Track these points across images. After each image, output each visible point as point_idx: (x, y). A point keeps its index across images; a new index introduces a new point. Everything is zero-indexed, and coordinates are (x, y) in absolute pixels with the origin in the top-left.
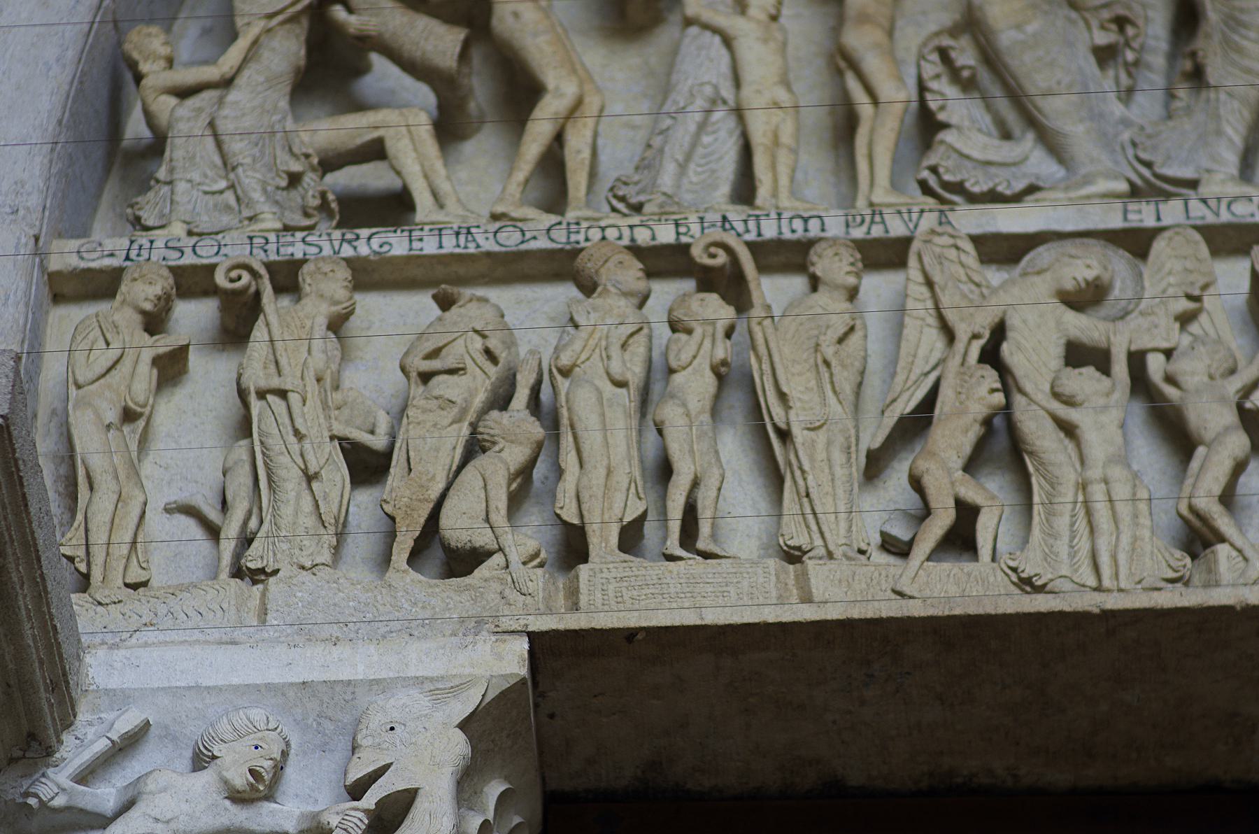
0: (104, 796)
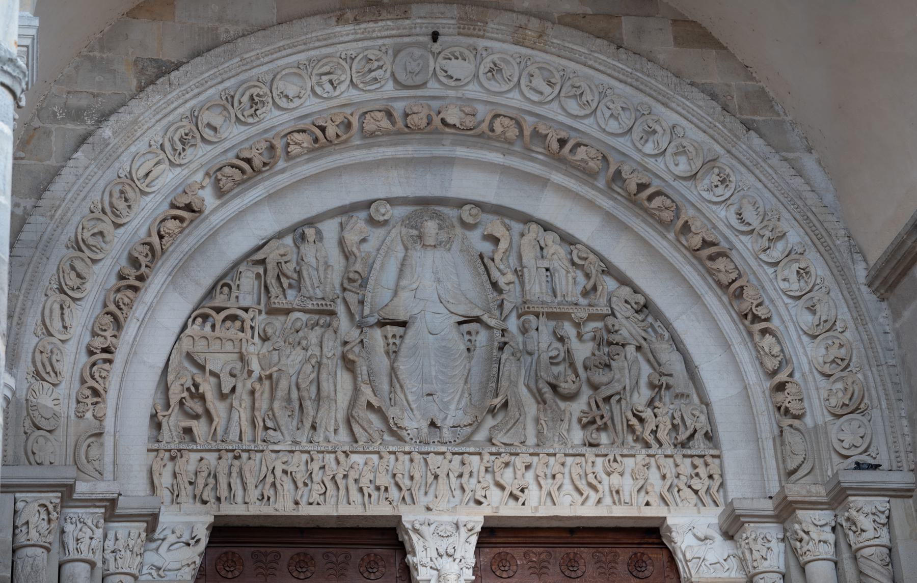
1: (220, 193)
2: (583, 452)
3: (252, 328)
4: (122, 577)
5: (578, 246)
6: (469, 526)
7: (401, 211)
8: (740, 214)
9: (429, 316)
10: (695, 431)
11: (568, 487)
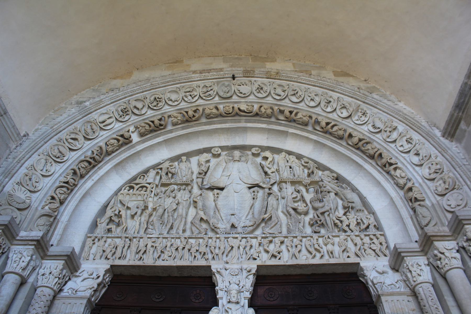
0: (81, 275)
1: (142, 135)
2: (312, 235)
3: (152, 191)
5: (304, 159)
6: (248, 269)
11: (304, 251)
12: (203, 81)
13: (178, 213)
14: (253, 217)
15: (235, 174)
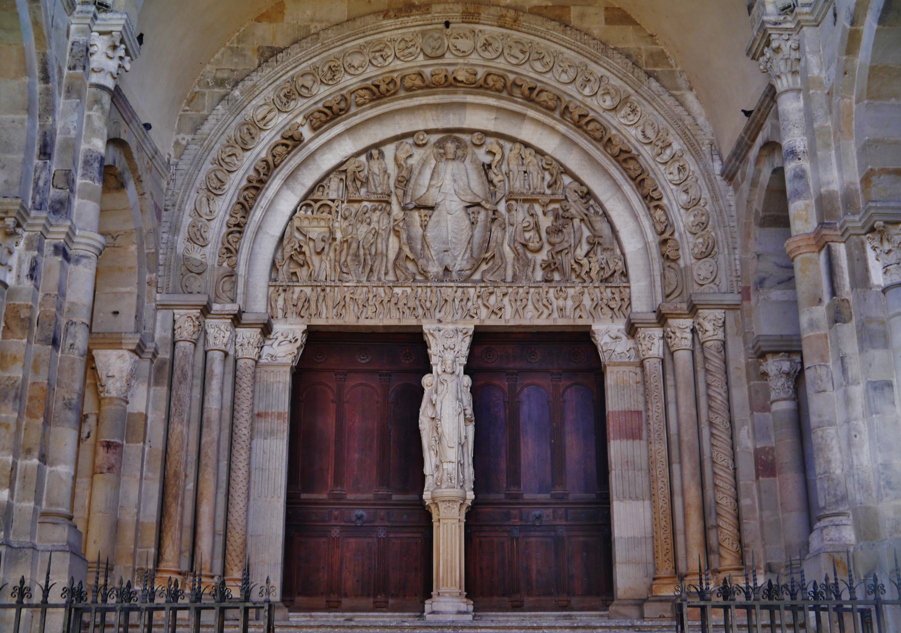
1: (314, 129)
3: (337, 212)
4: (246, 360)
5: (546, 157)
6: (464, 331)
7: (434, 138)
8: (644, 132)
9: (447, 203)
10: (615, 272)
11: (530, 306)
12: (400, 31)
13: (376, 249)
14: (472, 254)
15: (448, 184)
